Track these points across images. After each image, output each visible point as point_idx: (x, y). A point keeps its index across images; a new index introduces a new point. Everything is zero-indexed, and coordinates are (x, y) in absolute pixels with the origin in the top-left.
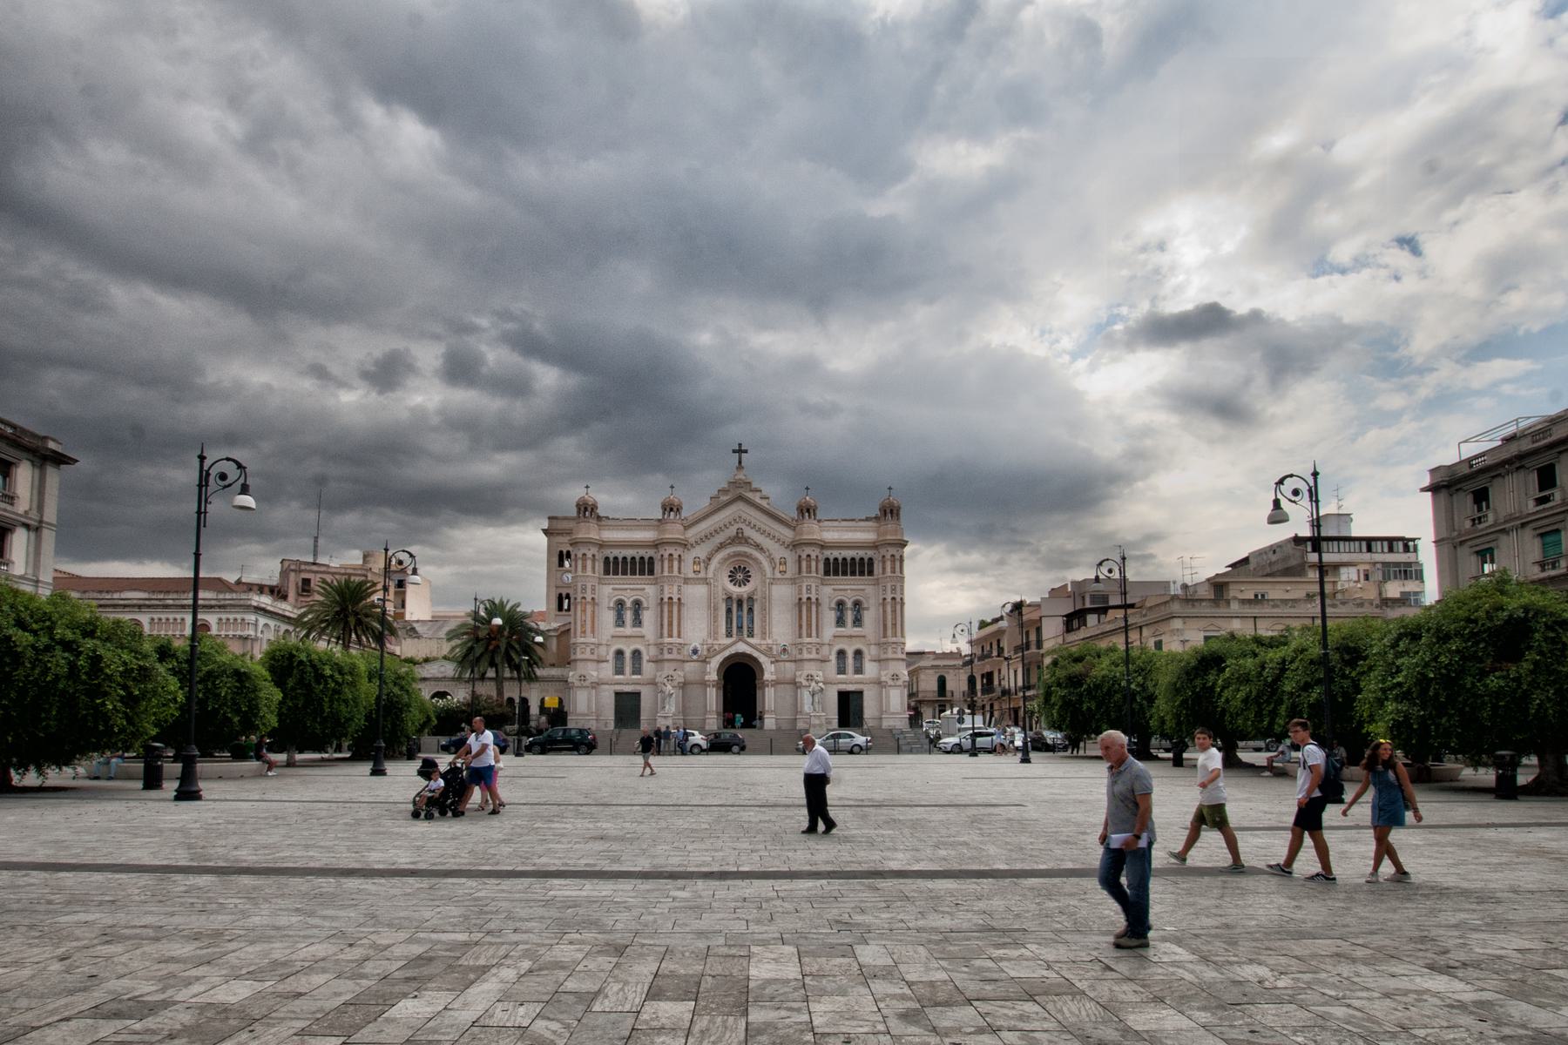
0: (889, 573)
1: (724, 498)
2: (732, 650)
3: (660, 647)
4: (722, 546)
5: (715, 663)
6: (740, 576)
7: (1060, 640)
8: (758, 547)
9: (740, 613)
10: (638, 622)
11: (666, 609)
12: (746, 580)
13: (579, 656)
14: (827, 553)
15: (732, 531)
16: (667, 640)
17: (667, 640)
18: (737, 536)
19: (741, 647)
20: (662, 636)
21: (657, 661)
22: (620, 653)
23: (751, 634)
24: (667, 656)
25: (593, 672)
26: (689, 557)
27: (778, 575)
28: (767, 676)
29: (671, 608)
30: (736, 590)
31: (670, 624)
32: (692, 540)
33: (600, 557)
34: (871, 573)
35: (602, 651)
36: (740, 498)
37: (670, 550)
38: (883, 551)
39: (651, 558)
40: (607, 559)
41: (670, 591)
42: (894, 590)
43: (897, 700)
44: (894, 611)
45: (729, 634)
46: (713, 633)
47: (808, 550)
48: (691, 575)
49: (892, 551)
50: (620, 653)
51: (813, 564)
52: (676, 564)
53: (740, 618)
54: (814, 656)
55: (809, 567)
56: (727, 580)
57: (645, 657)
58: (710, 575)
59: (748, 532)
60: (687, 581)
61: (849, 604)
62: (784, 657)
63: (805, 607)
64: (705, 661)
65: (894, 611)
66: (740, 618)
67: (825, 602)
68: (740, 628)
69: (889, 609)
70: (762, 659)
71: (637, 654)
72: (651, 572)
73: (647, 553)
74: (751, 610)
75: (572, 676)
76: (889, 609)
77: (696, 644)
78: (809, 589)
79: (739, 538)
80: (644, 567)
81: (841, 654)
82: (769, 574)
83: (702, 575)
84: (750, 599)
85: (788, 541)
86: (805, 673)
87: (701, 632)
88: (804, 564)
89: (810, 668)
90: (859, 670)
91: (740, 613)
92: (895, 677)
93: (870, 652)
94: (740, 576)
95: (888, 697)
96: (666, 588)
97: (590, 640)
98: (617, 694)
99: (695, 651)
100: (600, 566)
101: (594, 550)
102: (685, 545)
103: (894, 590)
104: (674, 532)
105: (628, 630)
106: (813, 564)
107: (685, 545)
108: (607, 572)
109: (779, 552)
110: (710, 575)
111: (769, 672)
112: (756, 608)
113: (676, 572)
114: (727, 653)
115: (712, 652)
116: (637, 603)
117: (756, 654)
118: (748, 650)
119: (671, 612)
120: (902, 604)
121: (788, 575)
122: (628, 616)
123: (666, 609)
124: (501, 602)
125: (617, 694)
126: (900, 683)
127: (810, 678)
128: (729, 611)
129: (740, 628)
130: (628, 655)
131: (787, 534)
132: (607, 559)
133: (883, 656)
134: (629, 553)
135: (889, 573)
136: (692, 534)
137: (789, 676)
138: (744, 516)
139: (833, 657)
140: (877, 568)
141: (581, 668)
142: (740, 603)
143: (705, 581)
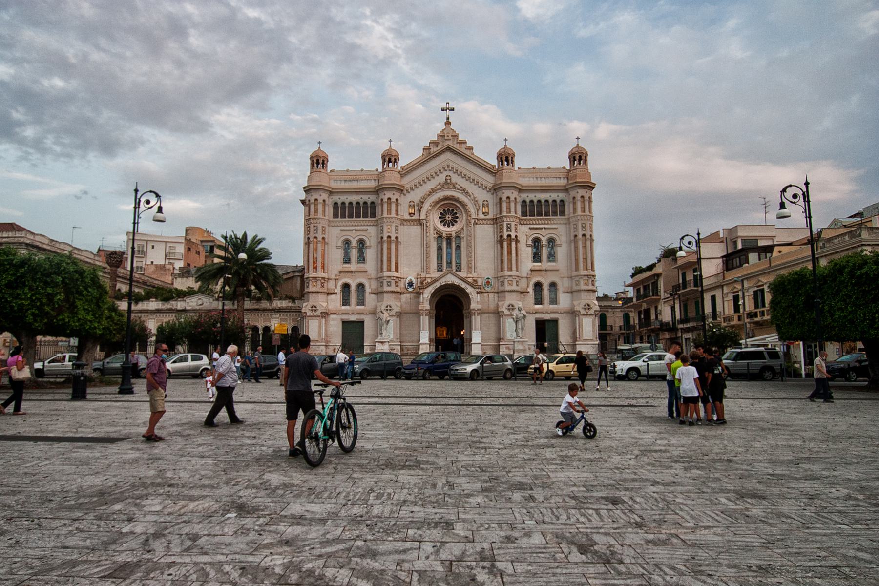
0: (579, 213)
1: (434, 150)
2: (443, 282)
3: (379, 280)
4: (433, 191)
5: (427, 293)
6: (449, 217)
7: (721, 276)
8: (464, 191)
9: (449, 247)
10: (362, 259)
11: (385, 246)
12: (453, 222)
13: (311, 289)
14: (524, 196)
15: (441, 179)
16: (386, 274)
17: (386, 274)
18: (446, 182)
19: (451, 279)
20: (382, 271)
21: (378, 293)
22: (346, 286)
23: (459, 269)
24: (386, 288)
25: (322, 303)
26: (404, 201)
27: (482, 216)
28: (473, 306)
29: (388, 243)
30: (445, 230)
31: (389, 260)
32: (407, 187)
33: (330, 202)
34: (563, 213)
35: (331, 285)
36: (449, 149)
37: (388, 194)
38: (573, 193)
39: (373, 203)
40: (336, 203)
41: (389, 230)
42: (584, 227)
43: (589, 328)
44: (585, 247)
45: (440, 269)
46: (426, 268)
47: (507, 193)
48: (407, 217)
49: (582, 192)
50: (346, 286)
51: (512, 205)
52: (393, 206)
53: (449, 254)
54: (514, 287)
55: (509, 208)
56: (437, 222)
57: (368, 290)
58: (423, 217)
59: (455, 179)
60: (403, 222)
61: (544, 241)
62: (488, 289)
63: (504, 242)
64: (418, 294)
65: (585, 247)
66: (449, 254)
67: (522, 239)
68: (449, 263)
69: (580, 245)
70: (469, 290)
71: (361, 286)
72: (373, 215)
73: (369, 198)
74: (458, 248)
75: (306, 307)
76: (580, 245)
77: (412, 277)
78: (509, 228)
79: (448, 184)
80: (366, 210)
81: (538, 286)
82: (473, 217)
83: (416, 217)
84: (458, 237)
85: (490, 185)
86: (507, 303)
87: (414, 262)
88: (504, 205)
89: (511, 299)
90: (554, 301)
91: (449, 247)
92: (588, 307)
93: (563, 285)
94: (449, 217)
95: (581, 326)
96: (385, 228)
97: (320, 274)
98: (344, 323)
99: (410, 284)
100: (330, 210)
101: (325, 196)
102: (401, 190)
103: (584, 227)
104: (392, 178)
105: (353, 266)
106: (512, 205)
107: (401, 190)
108: (335, 215)
109: (482, 195)
110: (423, 217)
111: (476, 301)
112: (463, 244)
113: (393, 215)
114: (438, 285)
115: (423, 285)
116: (361, 242)
117: (463, 285)
118: (457, 281)
119: (389, 249)
120: (592, 240)
121: (490, 216)
122: (354, 254)
123: (385, 246)
124: (240, 236)
125: (344, 323)
126: (592, 312)
127: (511, 307)
128: (440, 249)
129: (449, 263)
130: (353, 287)
131: (489, 180)
132: (336, 203)
133: (575, 288)
134: (354, 199)
135: (579, 213)
136: (406, 182)
137: (492, 307)
138: (451, 164)
139: (531, 289)
140: (568, 209)
141: (313, 300)
142: (449, 239)
143: (419, 222)
